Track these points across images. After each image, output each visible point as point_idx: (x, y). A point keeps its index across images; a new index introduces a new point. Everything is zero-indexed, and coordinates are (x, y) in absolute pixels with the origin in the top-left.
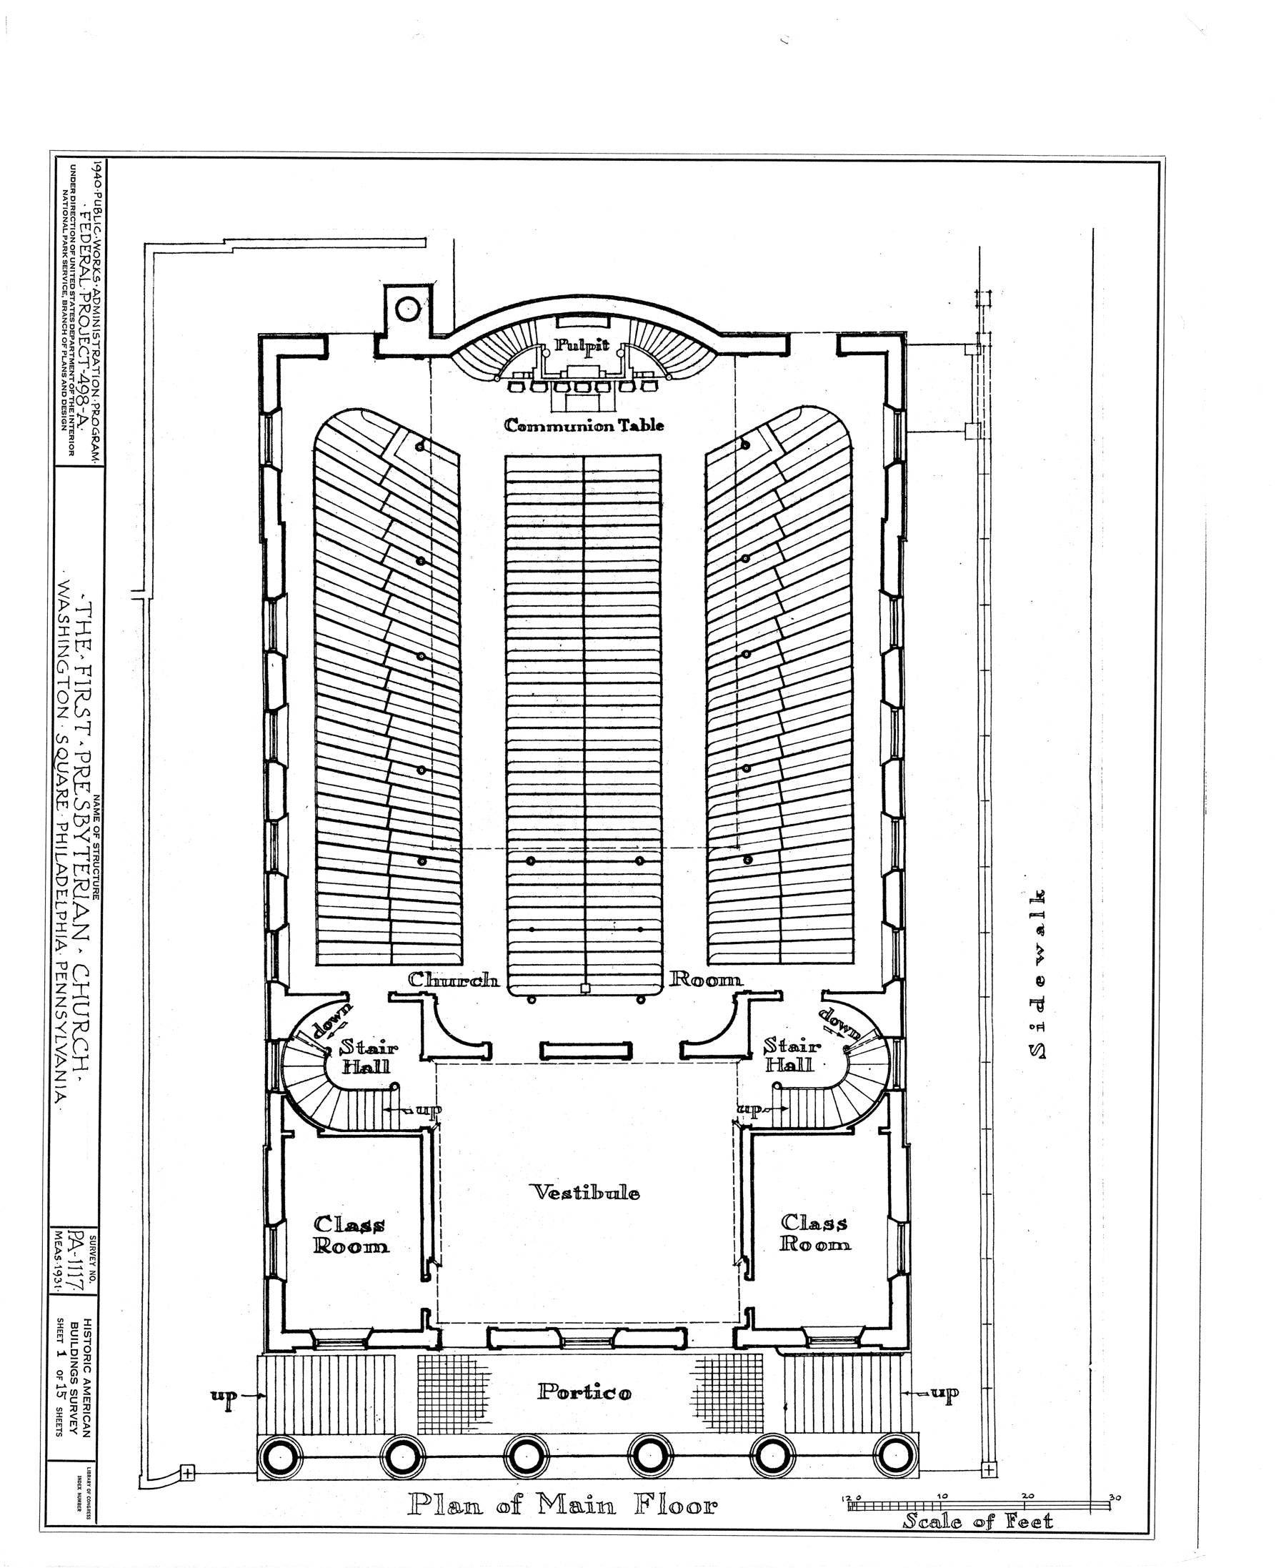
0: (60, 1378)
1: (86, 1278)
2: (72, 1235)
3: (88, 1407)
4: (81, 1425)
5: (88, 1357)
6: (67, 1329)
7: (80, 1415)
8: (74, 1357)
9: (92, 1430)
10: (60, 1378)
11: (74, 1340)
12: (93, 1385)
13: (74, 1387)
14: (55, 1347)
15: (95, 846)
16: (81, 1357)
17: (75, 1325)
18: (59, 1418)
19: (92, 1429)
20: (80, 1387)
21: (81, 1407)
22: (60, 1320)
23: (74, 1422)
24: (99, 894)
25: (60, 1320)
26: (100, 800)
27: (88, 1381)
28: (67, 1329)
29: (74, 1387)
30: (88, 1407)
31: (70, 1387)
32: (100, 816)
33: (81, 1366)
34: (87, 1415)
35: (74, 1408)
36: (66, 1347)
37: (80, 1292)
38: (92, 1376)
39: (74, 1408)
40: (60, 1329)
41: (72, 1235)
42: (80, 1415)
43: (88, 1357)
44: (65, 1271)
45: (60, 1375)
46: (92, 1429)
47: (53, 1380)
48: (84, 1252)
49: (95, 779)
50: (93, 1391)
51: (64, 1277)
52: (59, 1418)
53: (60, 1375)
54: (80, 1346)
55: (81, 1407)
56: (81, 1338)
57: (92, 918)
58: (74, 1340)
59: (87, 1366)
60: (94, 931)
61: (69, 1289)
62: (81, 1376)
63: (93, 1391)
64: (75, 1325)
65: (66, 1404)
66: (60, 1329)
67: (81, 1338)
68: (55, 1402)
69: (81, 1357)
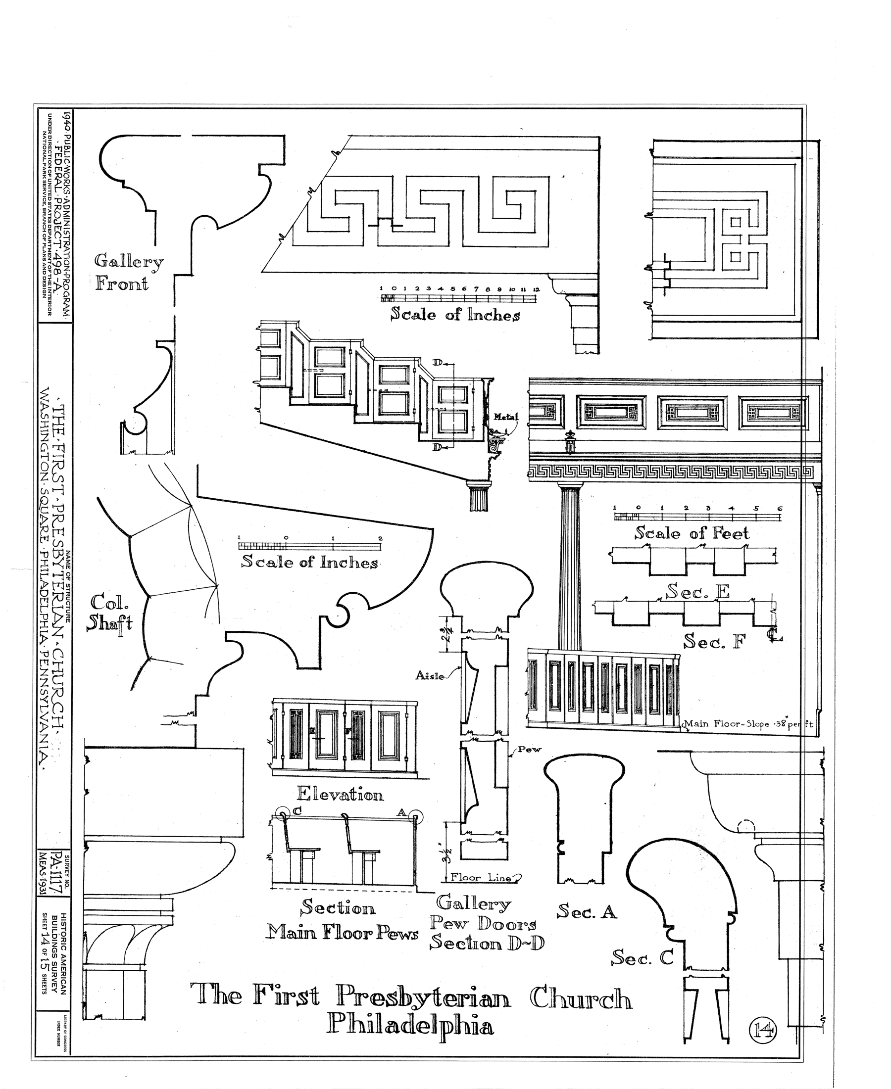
0: (46, 954)
1: (63, 884)
3: (64, 974)
4: (59, 986)
5: (64, 939)
6: (50, 920)
7: (59, 979)
8: (55, 939)
10: (46, 954)
11: (55, 928)
12: (68, 958)
13: (55, 960)
15: (68, 585)
16: (59, 939)
17: (55, 918)
18: (44, 981)
19: (67, 989)
20: (58, 960)
21: (59, 974)
22: (45, 914)
23: (55, 984)
25: (45, 914)
27: (64, 956)
28: (50, 920)
29: (55, 960)
30: (64, 974)
31: (52, 960)
33: (59, 946)
34: (63, 979)
35: (55, 975)
37: (60, 894)
39: (55, 975)
40: (45, 920)
41: (54, 856)
42: (59, 979)
43: (64, 939)
45: (45, 952)
46: (67, 989)
47: (40, 955)
48: (62, 867)
50: (68, 963)
52: (44, 981)
53: (45, 952)
54: (59, 931)
56: (59, 926)
58: (55, 928)
59: (63, 946)
62: (60, 952)
63: (68, 963)
64: (55, 918)
66: (45, 920)
67: (59, 926)
68: (40, 972)
69: (59, 939)
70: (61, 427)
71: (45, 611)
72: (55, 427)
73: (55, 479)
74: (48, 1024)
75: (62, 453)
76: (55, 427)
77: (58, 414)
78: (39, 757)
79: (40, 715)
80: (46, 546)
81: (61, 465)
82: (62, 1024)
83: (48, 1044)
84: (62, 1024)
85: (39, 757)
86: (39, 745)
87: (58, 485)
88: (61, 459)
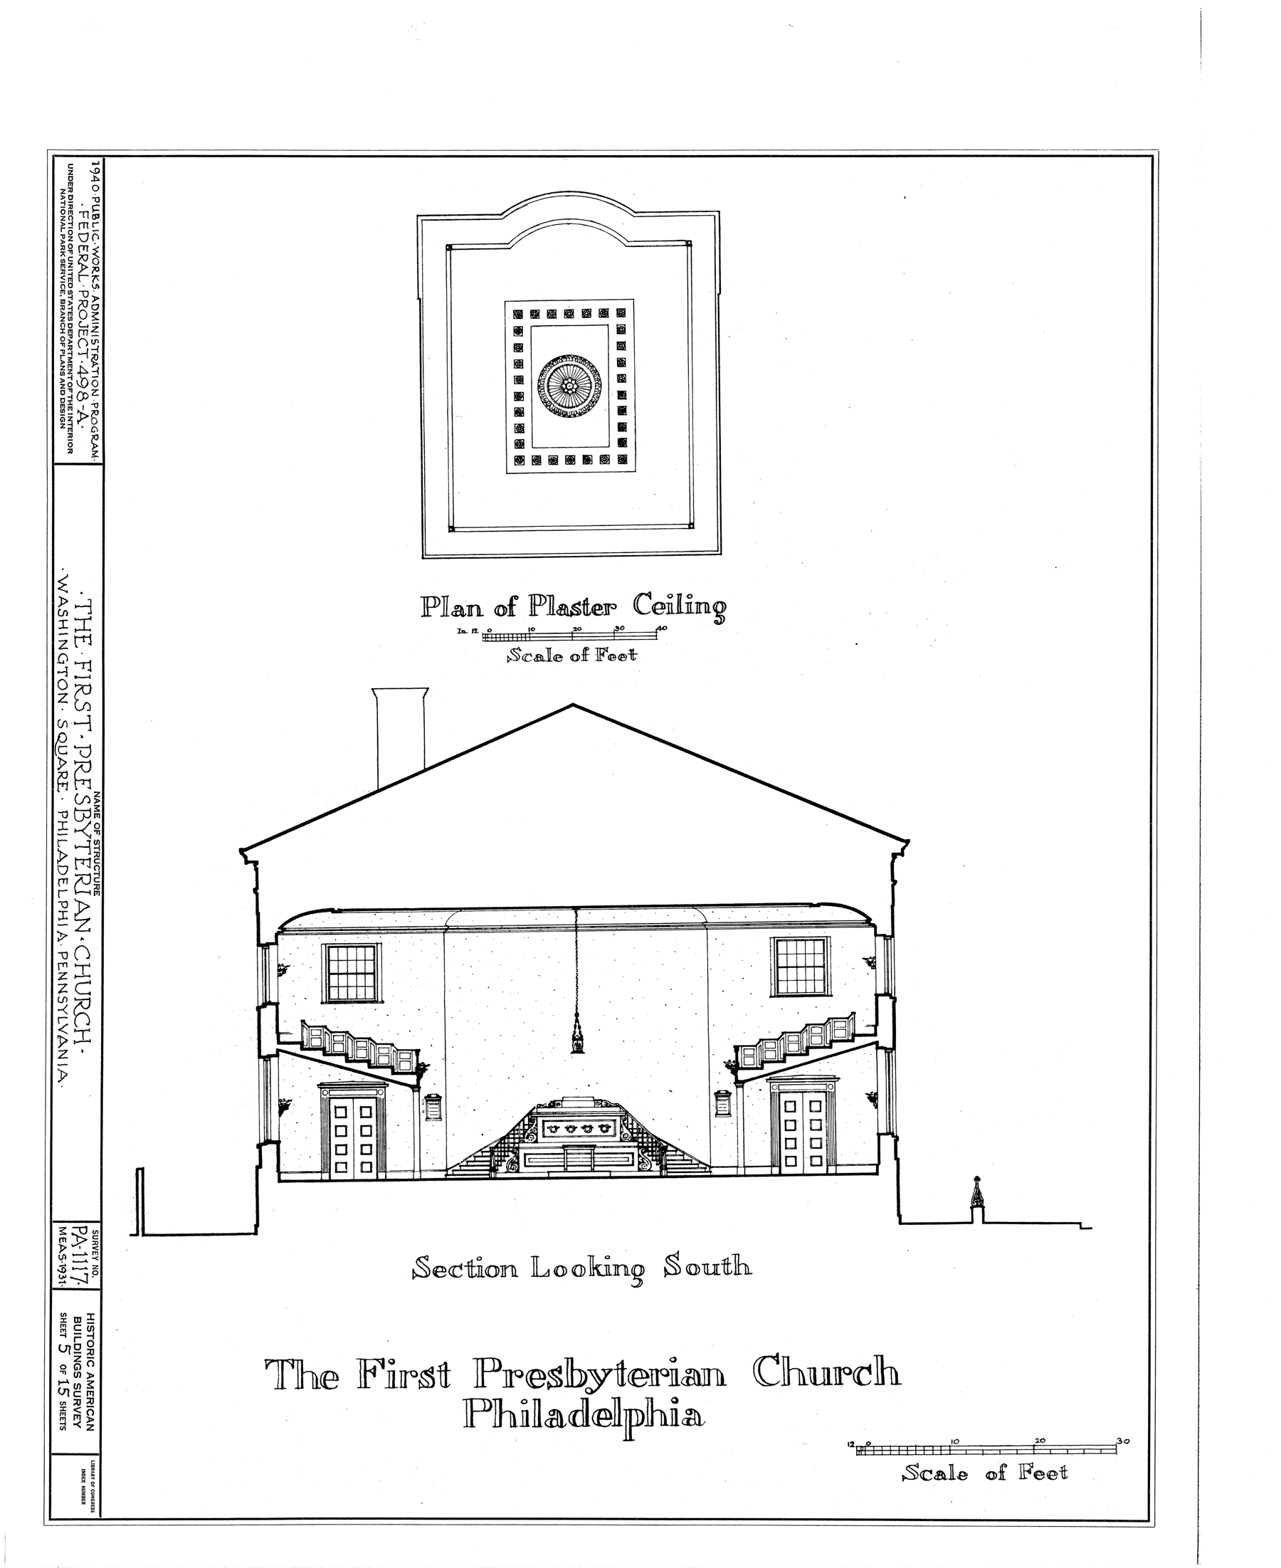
1: (90, 1271)
2: (76, 1231)
3: (91, 1401)
4: (84, 1419)
6: (70, 1323)
7: (83, 1409)
8: (78, 1351)
9: (96, 1423)
11: (78, 1335)
12: (96, 1379)
13: (77, 1381)
14: (57, 1340)
16: (84, 1351)
17: (78, 1320)
18: (63, 1412)
19: (96, 1423)
20: (83, 1381)
21: (84, 1401)
22: (63, 1315)
25: (63, 1315)
28: (70, 1323)
29: (77, 1381)
30: (91, 1401)
31: (73, 1381)
33: (84, 1360)
34: (90, 1408)
35: (78, 1402)
39: (78, 1402)
40: (63, 1324)
41: (76, 1231)
42: (83, 1409)
44: (69, 1268)
45: (63, 1369)
47: (57, 1376)
48: (87, 1247)
52: (63, 1412)
53: (63, 1369)
54: (83, 1340)
55: (84, 1401)
56: (84, 1333)
58: (78, 1335)
59: (90, 1361)
61: (73, 1284)
62: (85, 1370)
63: (96, 1385)
64: (78, 1320)
65: (70, 1401)
66: (63, 1324)
67: (84, 1333)
68: (57, 1399)
69: (84, 1351)
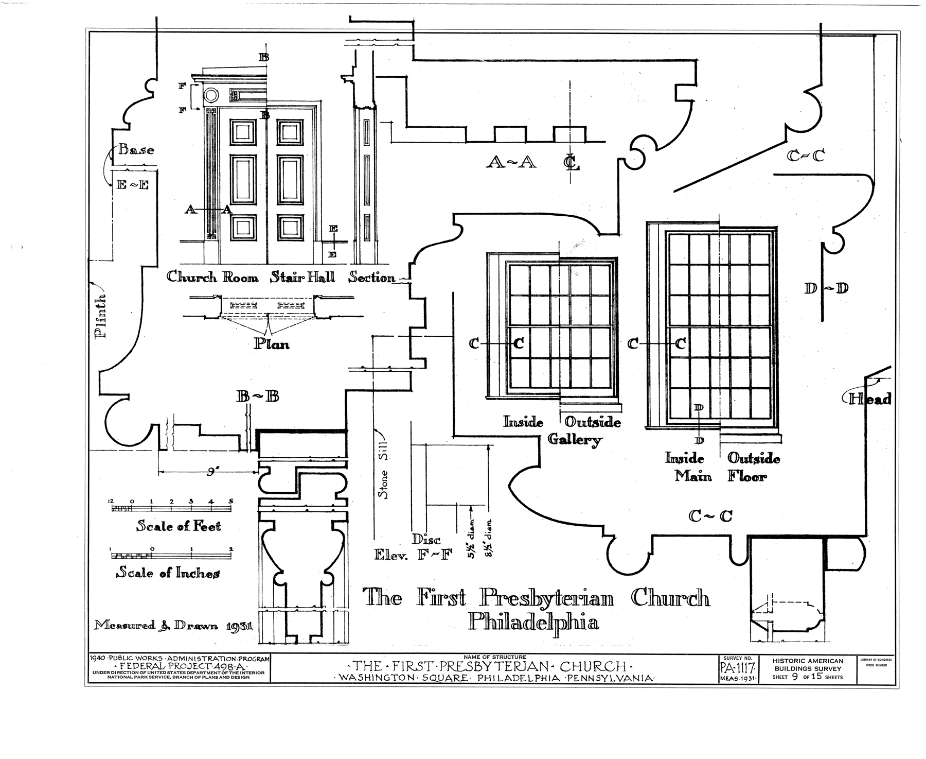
1: (748, 661)
2: (724, 669)
3: (825, 661)
4: (836, 665)
5: (796, 661)
8: (795, 669)
9: (839, 658)
11: (786, 669)
12: (812, 657)
13: (813, 669)
15: (494, 658)
16: (795, 665)
17: (777, 669)
18: (832, 677)
19: (838, 658)
20: (813, 665)
21: (825, 665)
22: (774, 677)
23: (834, 669)
24: (523, 655)
25: (774, 677)
26: (467, 655)
29: (813, 669)
30: (825, 661)
31: (813, 671)
32: (476, 655)
33: (801, 665)
34: (830, 661)
35: (826, 668)
36: (790, 674)
37: (756, 666)
38: (807, 658)
39: (826, 668)
40: (779, 677)
41: (724, 669)
43: (796, 661)
44: (744, 675)
45: (806, 677)
48: (734, 663)
49: (455, 658)
50: (816, 658)
51: (748, 675)
52: (832, 677)
53: (806, 677)
54: (789, 665)
55: (825, 665)
56: (784, 665)
57: (537, 659)
58: (786, 669)
59: (801, 661)
60: (544, 659)
62: (807, 664)
63: (816, 658)
64: (777, 669)
65: (825, 673)
66: (779, 677)
67: (784, 665)
68: (823, 681)
69: (795, 665)
70: (373, 664)
71: (533, 678)
72: (373, 669)
73: (419, 668)
74: (868, 674)
75: (401, 664)
76: (373, 669)
77: (361, 665)
78: (647, 682)
79: (617, 681)
80: (472, 677)
81: (410, 664)
82: (868, 662)
83: (885, 675)
84: (868, 662)
85: (647, 682)
86: (641, 682)
87: (425, 666)
88: (405, 664)
